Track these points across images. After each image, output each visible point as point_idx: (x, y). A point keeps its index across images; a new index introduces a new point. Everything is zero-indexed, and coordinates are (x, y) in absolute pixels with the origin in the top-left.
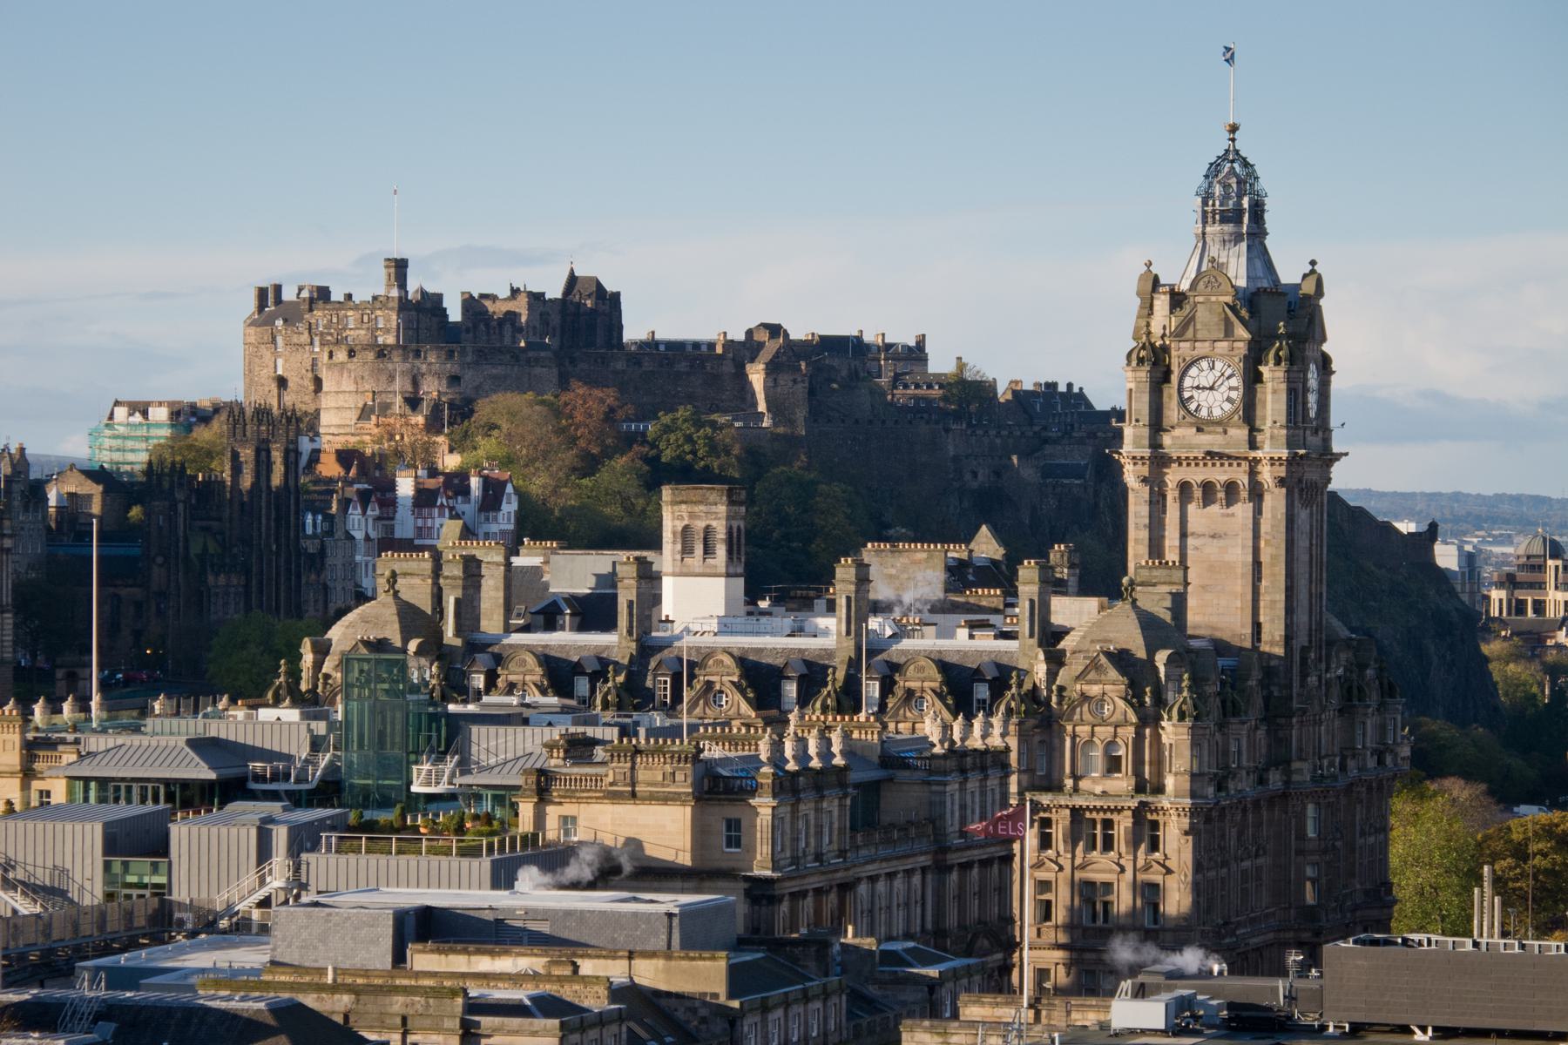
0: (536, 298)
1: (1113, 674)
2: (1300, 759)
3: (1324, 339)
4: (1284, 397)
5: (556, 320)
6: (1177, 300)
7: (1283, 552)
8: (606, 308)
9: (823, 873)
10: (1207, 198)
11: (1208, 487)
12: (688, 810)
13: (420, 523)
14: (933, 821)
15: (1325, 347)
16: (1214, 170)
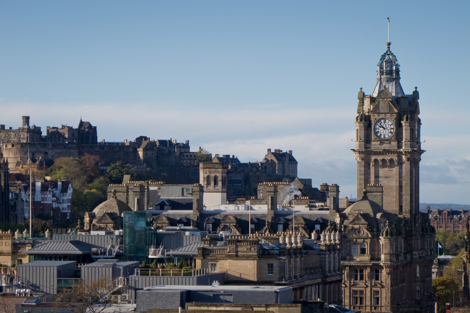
0: (70, 129)
1: (363, 221)
2: (414, 251)
3: (419, 113)
4: (409, 131)
5: (76, 135)
6: (373, 100)
7: (409, 182)
8: (92, 131)
9: (298, 283)
10: (381, 68)
11: (383, 161)
12: (256, 261)
13: (43, 196)
14: (322, 267)
15: (419, 116)
16: (383, 57)
